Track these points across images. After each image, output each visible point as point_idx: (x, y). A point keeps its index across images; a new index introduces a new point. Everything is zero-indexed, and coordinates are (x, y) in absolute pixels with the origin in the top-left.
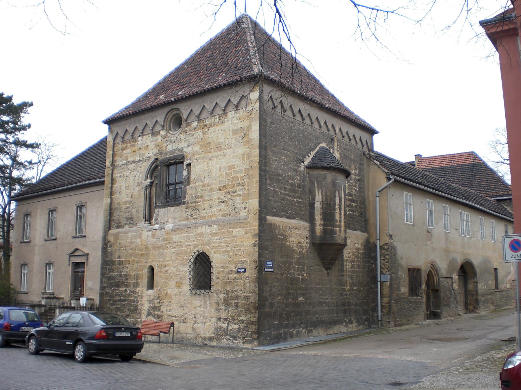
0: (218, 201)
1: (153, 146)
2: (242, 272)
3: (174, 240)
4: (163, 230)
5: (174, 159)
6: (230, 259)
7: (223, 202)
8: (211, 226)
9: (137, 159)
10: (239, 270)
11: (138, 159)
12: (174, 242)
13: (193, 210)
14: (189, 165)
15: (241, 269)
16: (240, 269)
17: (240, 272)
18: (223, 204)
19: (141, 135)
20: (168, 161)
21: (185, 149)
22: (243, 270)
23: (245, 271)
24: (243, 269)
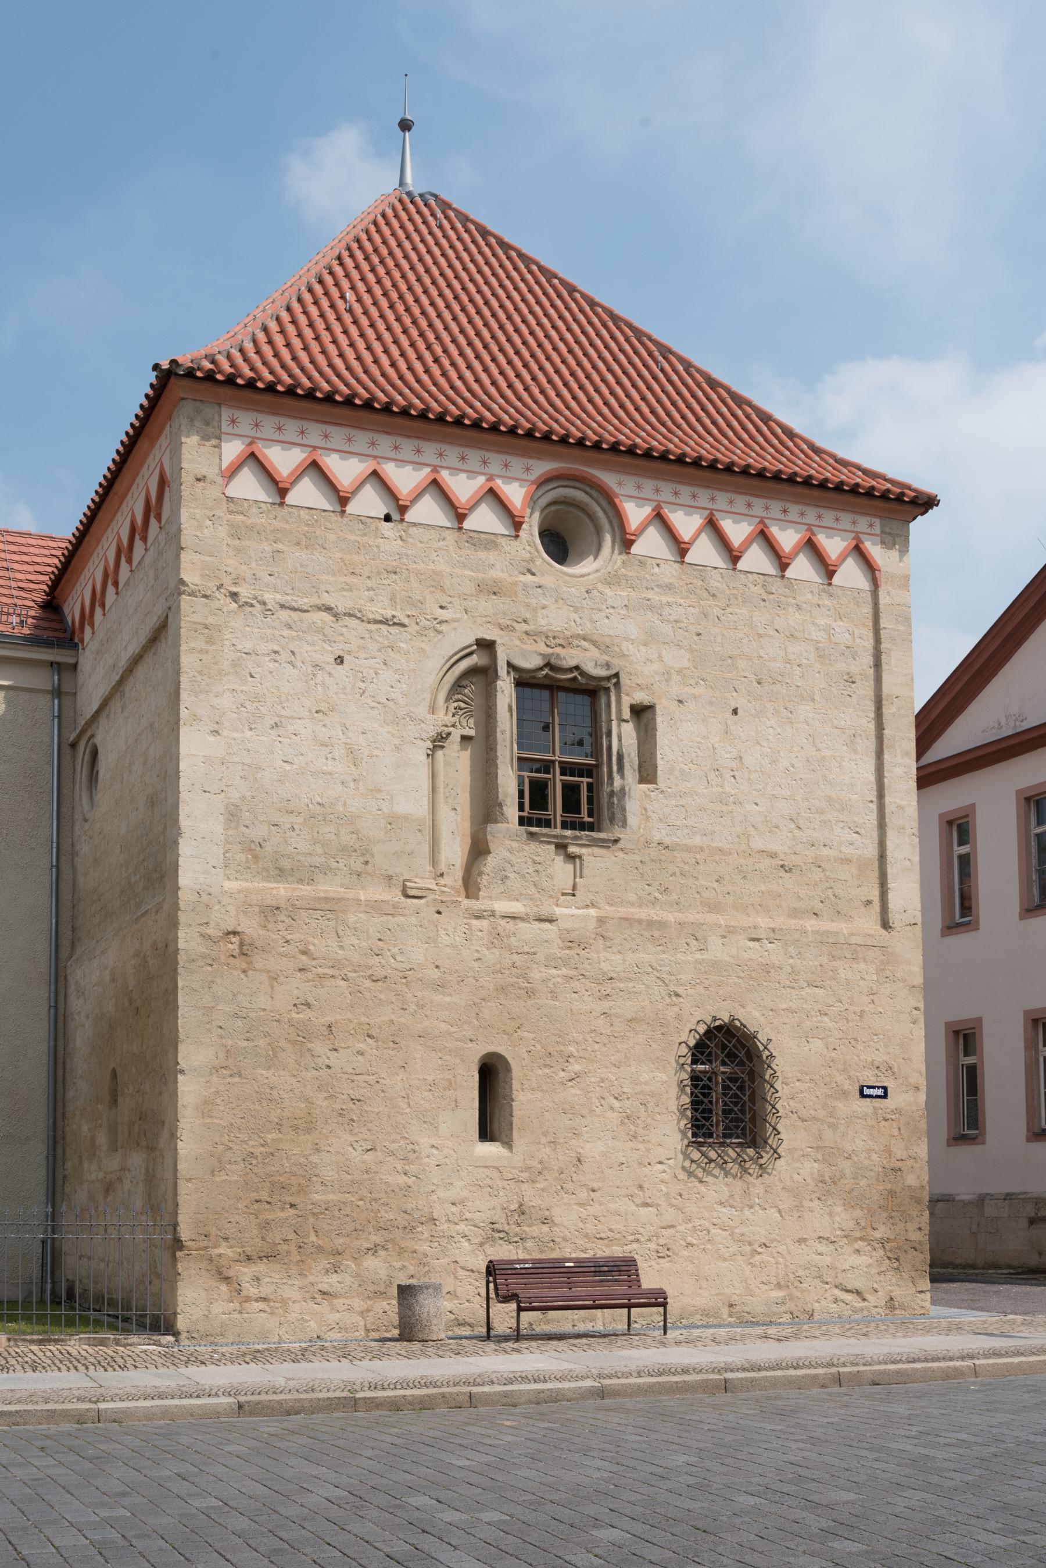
0: (768, 861)
1: (469, 588)
2: (877, 1097)
3: (606, 967)
4: (547, 925)
5: (570, 670)
6: (833, 1055)
7: (790, 871)
8: (758, 940)
9: (381, 609)
10: (866, 1091)
11: (389, 613)
12: (604, 974)
13: (674, 874)
14: (641, 713)
15: (873, 1087)
16: (869, 1087)
17: (870, 1096)
18: (788, 874)
19: (395, 516)
20: (541, 669)
21: (629, 648)
22: (880, 1092)
23: (885, 1096)
24: (879, 1087)
